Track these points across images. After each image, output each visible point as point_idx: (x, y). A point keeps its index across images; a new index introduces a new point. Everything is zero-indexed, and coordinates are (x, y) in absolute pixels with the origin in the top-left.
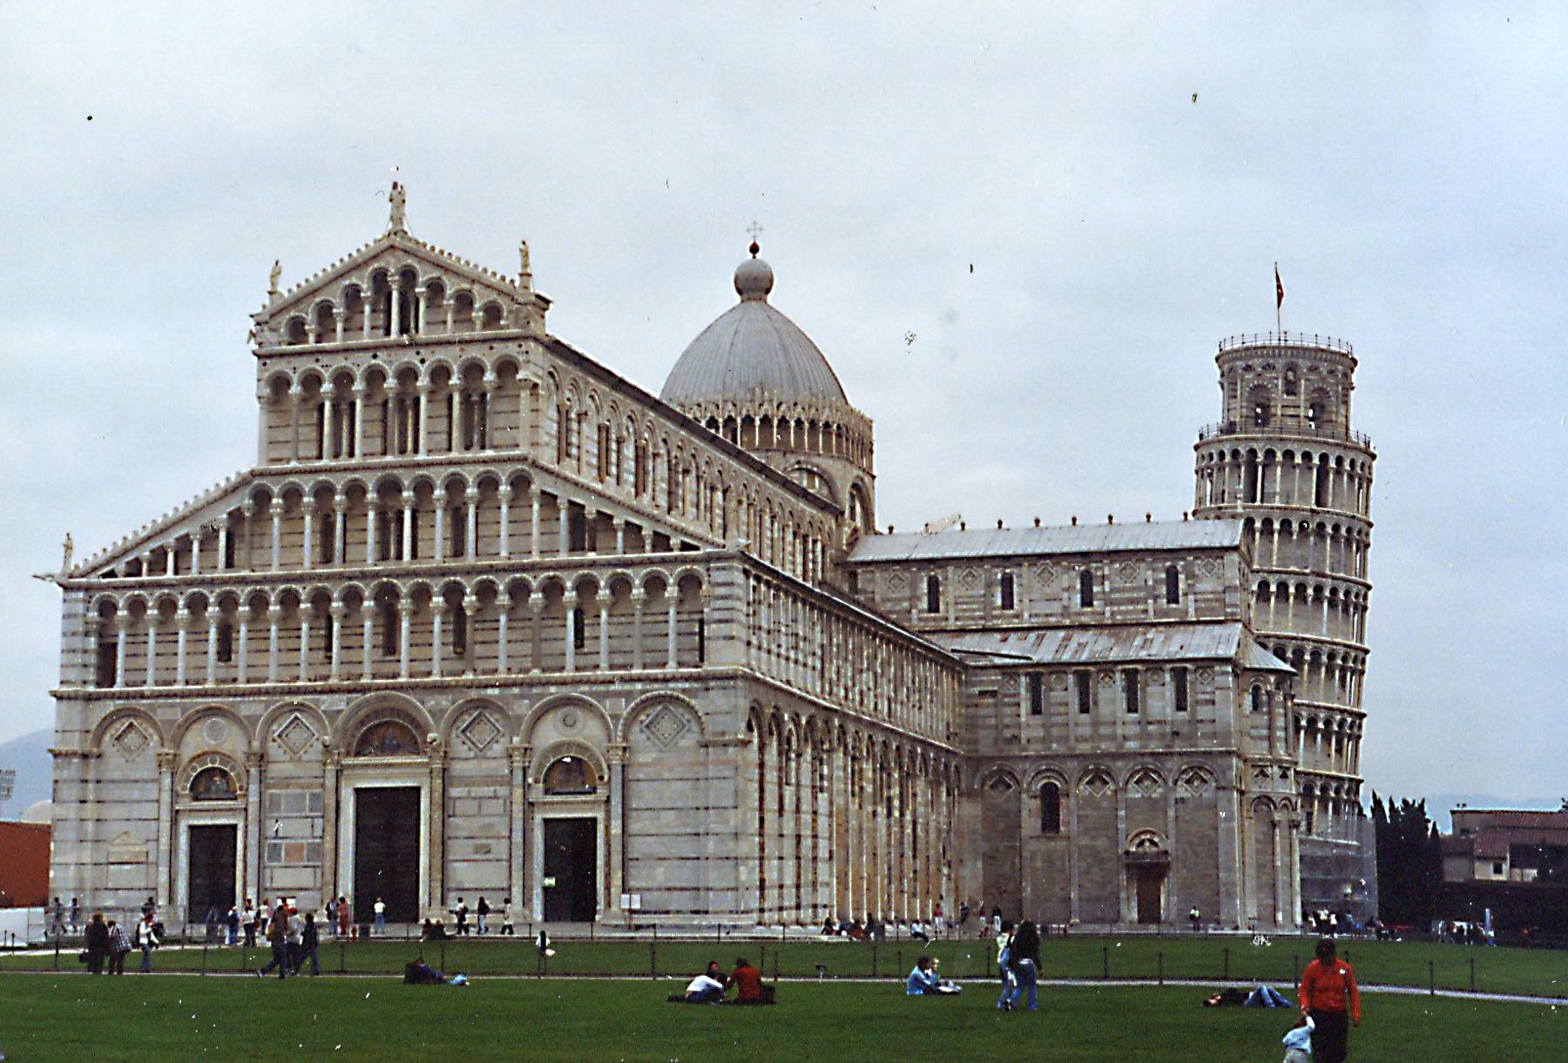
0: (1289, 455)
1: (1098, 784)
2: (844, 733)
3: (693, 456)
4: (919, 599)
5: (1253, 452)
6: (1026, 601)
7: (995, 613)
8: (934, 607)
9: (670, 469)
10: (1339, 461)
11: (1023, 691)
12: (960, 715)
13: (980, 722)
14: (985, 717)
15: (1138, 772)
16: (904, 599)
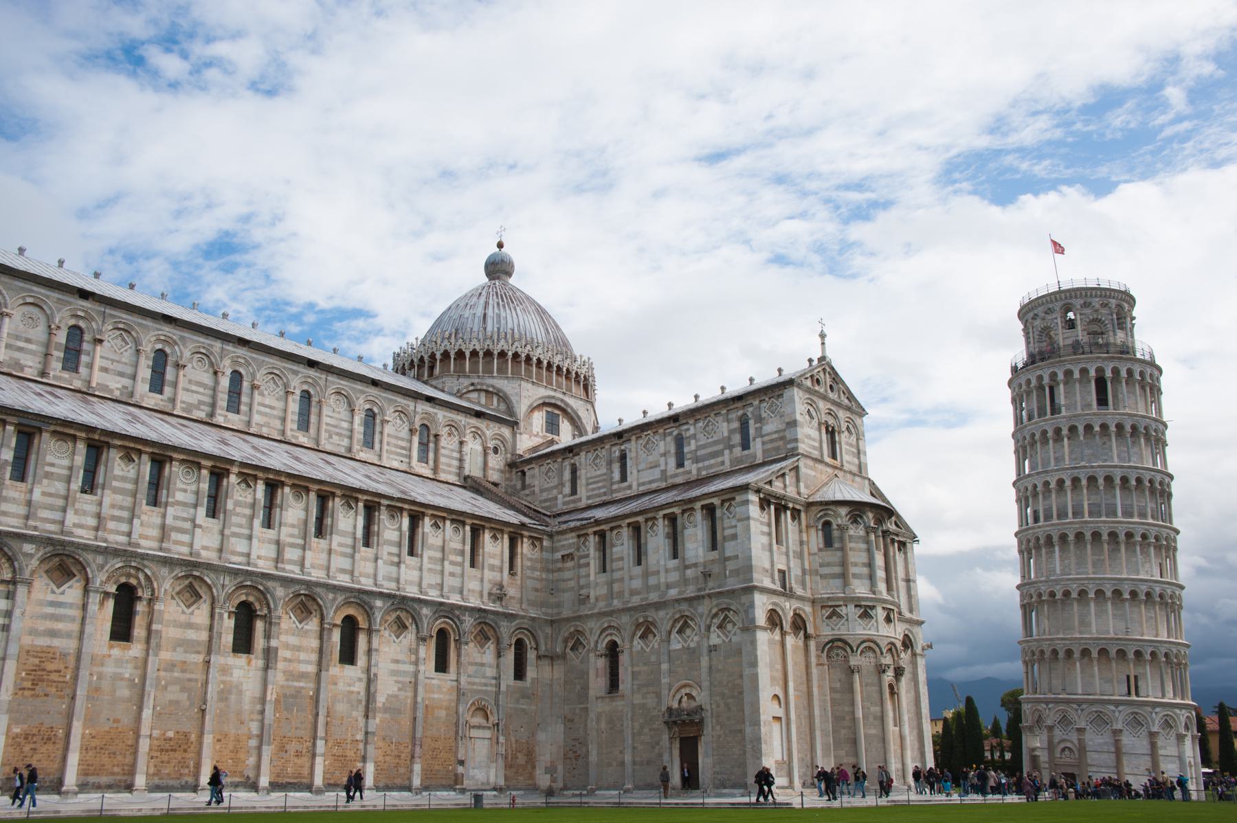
0: (1069, 373)
1: (650, 637)
2: (84, 569)
3: (129, 333)
4: (562, 484)
5: (1040, 378)
6: (635, 472)
7: (615, 487)
8: (574, 491)
9: (50, 334)
10: (1116, 371)
11: (592, 552)
12: (541, 580)
13: (562, 585)
14: (563, 581)
15: (676, 621)
16: (552, 488)
